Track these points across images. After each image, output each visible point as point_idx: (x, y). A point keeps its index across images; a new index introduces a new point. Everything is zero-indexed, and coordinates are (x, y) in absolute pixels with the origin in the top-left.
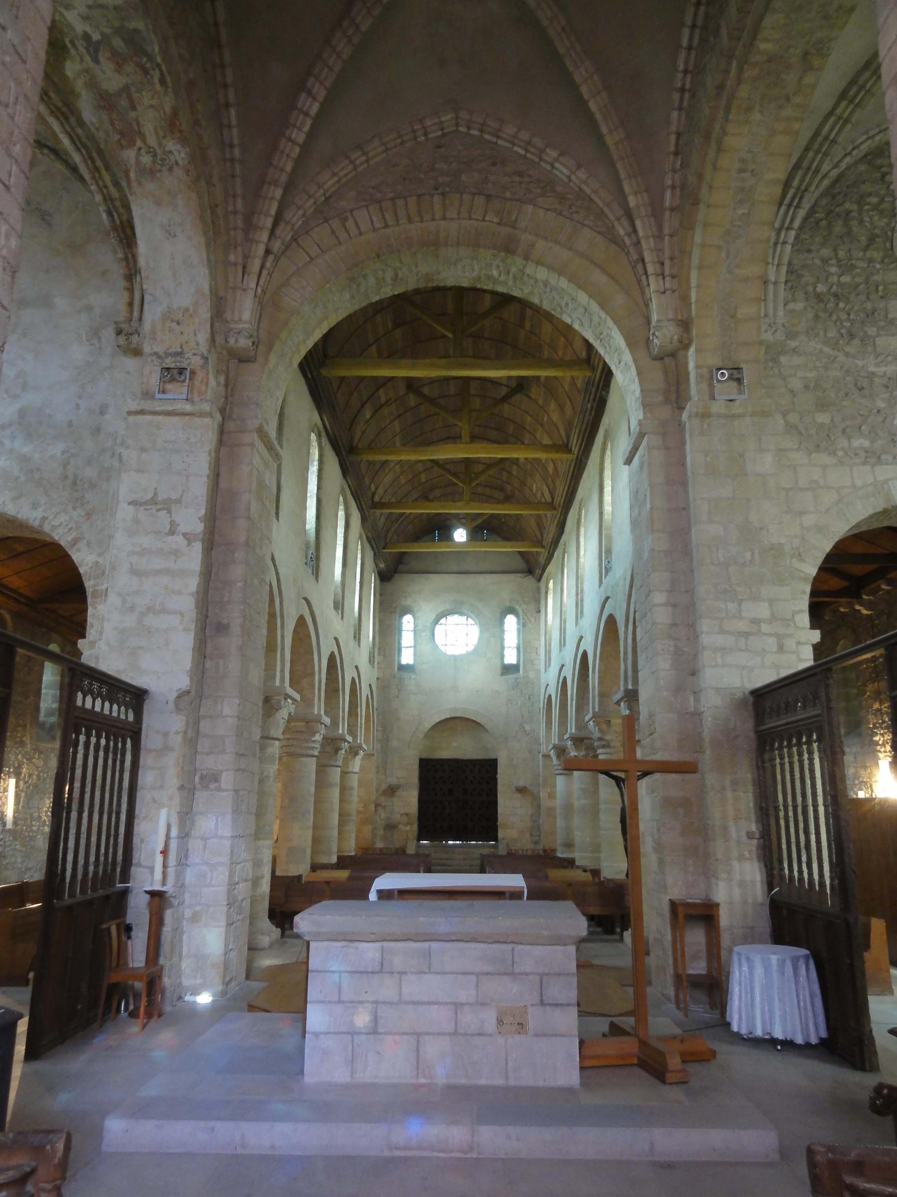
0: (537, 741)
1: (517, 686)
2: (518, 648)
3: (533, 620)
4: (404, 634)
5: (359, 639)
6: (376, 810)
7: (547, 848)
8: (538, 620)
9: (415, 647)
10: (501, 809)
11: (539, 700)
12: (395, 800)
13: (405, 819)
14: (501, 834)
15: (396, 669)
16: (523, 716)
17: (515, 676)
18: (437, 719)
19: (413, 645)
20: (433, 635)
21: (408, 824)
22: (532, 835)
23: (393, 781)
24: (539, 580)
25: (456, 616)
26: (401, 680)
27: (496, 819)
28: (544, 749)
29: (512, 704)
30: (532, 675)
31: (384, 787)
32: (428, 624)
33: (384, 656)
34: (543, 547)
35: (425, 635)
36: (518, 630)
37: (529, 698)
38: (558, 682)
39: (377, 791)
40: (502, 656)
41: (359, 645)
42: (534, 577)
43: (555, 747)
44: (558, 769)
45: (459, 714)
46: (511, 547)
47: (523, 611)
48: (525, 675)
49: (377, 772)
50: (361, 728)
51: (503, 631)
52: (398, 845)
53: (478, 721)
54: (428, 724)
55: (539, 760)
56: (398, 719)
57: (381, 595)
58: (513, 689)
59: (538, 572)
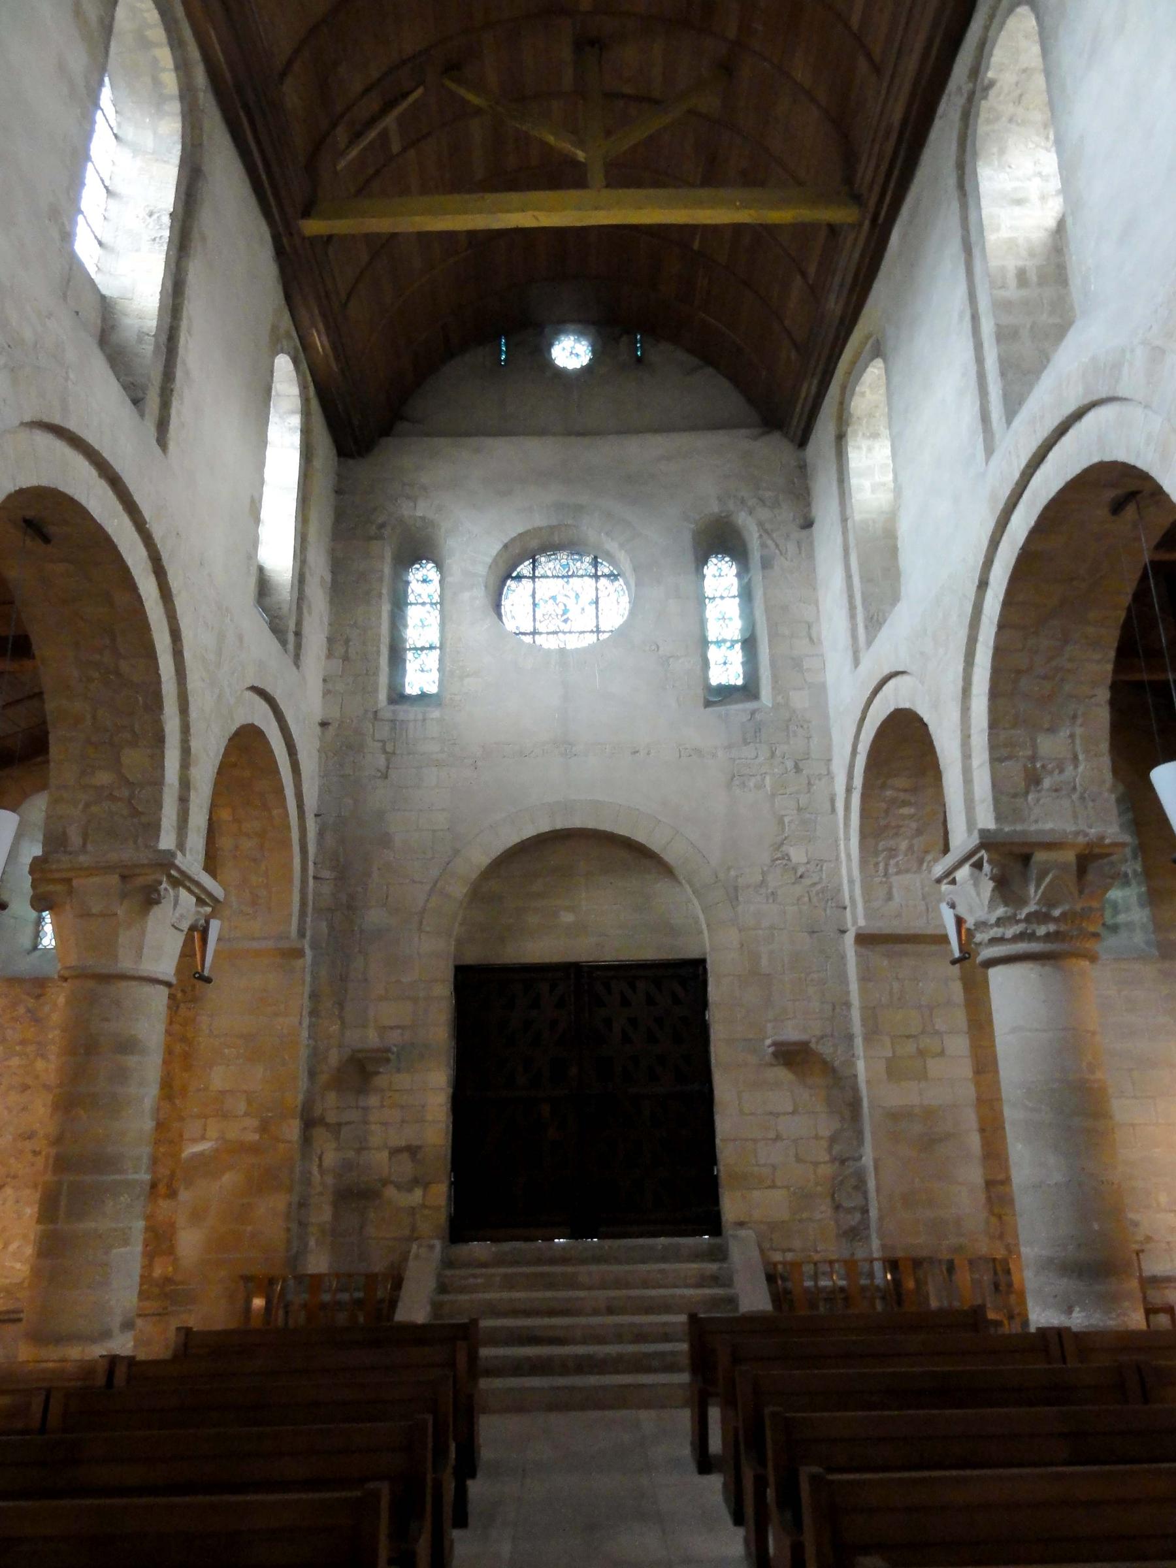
0: (832, 897)
1: (758, 730)
2: (749, 644)
3: (791, 548)
4: (414, 614)
5: (162, 426)
6: (306, 1140)
7: (900, 1254)
8: (807, 551)
9: (442, 647)
10: (724, 1125)
11: (830, 775)
12: (373, 1100)
13: (405, 1168)
14: (731, 1206)
15: (383, 696)
16: (781, 822)
17: (751, 705)
18: (511, 837)
19: (436, 641)
20: (497, 606)
21: (416, 1182)
22: (837, 1207)
23: (372, 1039)
24: (802, 442)
25: (563, 556)
26: (394, 723)
27: (710, 1156)
28: (857, 919)
29: (744, 784)
30: (800, 700)
31: (334, 1058)
32: (482, 570)
33: (346, 658)
34: (857, 199)
35: (477, 596)
36: (746, 594)
37: (798, 769)
38: (983, 584)
39: (312, 1074)
40: (706, 664)
41: (162, 441)
42: (786, 435)
43: (988, 842)
44: (994, 941)
45: (577, 822)
46: (746, 205)
47: (760, 524)
48: (779, 699)
49: (314, 1013)
50: (184, 800)
51: (701, 600)
52: (379, 1265)
53: (640, 837)
54: (480, 856)
55: (843, 957)
56: (385, 841)
57: (338, 492)
58: (746, 742)
59: (809, 388)
